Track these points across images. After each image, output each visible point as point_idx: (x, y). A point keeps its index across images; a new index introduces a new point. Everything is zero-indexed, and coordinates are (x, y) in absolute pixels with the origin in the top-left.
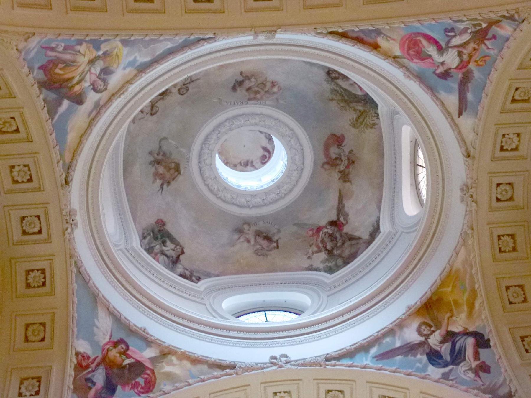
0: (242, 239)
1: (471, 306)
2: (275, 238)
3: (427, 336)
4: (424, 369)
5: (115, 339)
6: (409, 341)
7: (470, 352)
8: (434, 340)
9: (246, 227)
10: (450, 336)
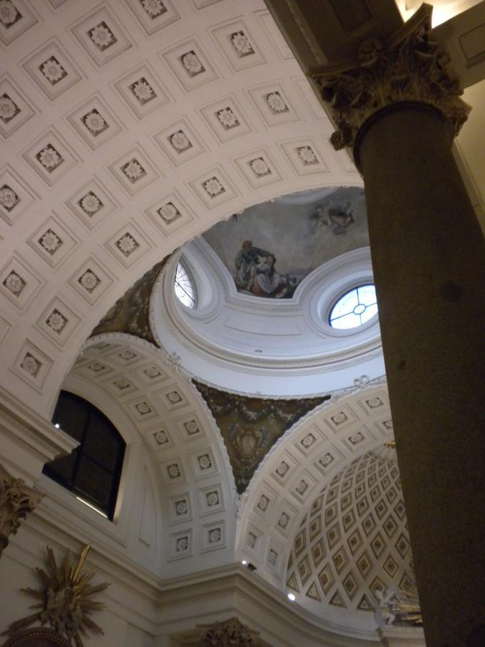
0: (320, 224)
2: (348, 212)
9: (319, 210)
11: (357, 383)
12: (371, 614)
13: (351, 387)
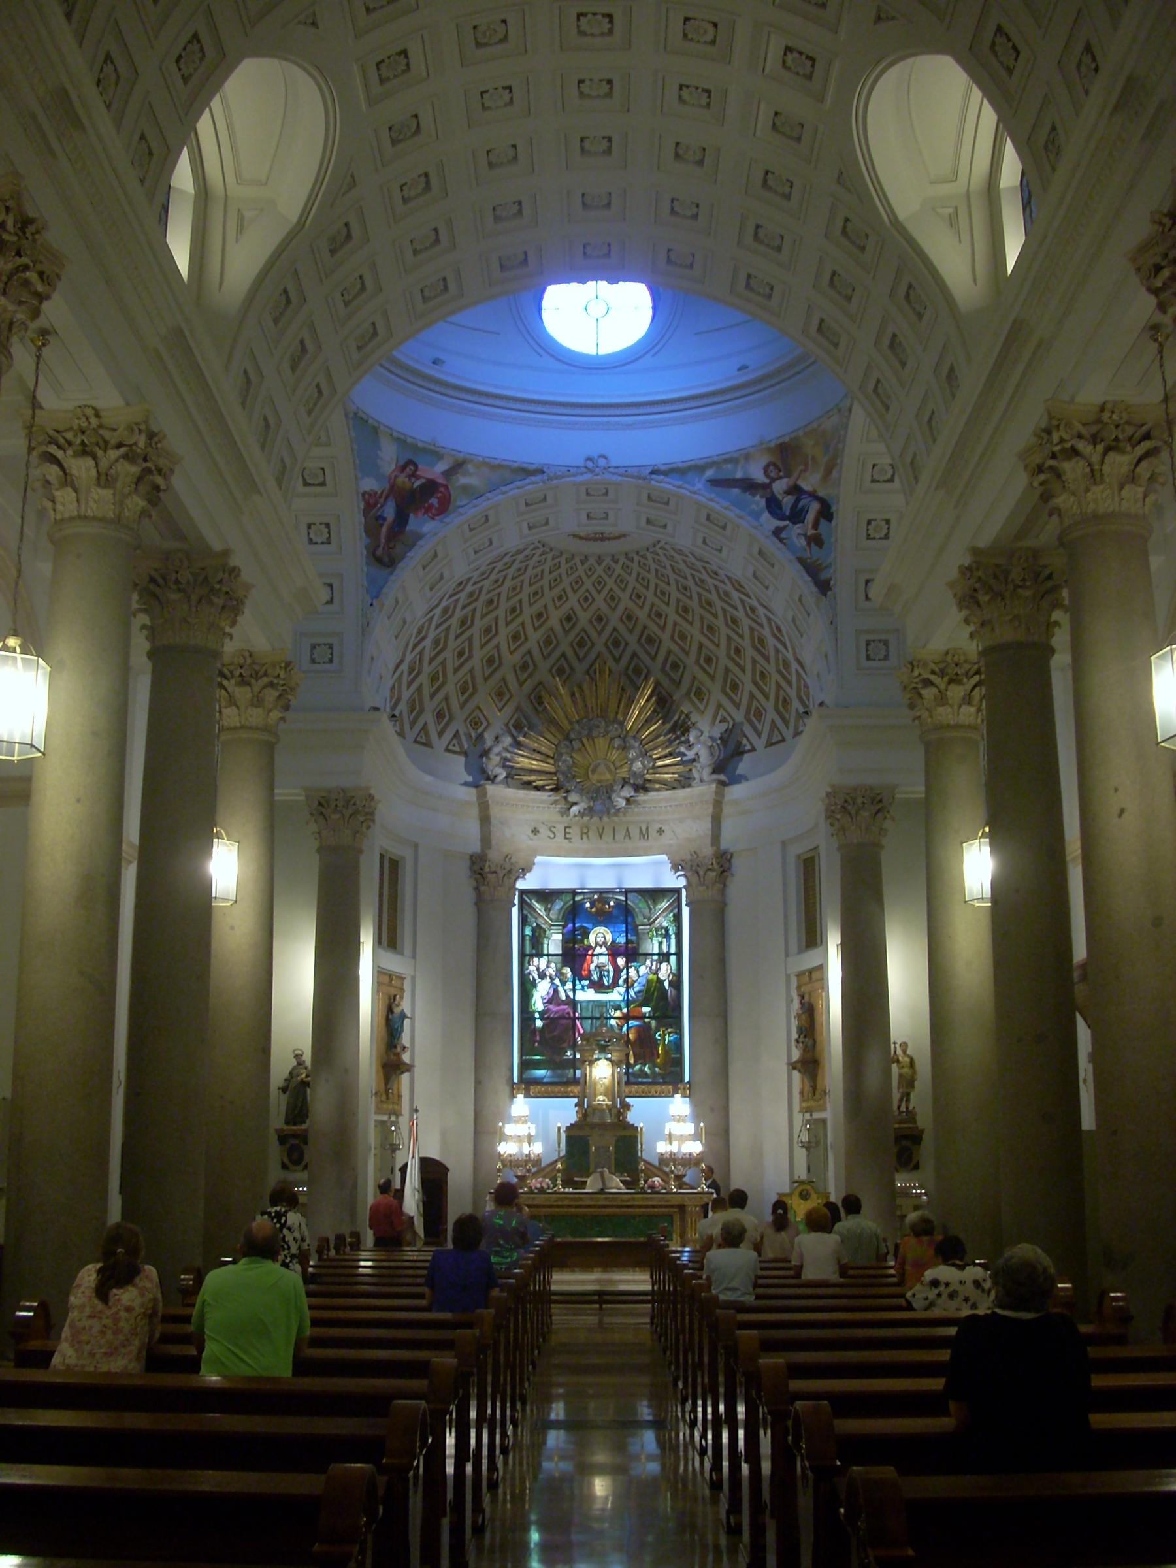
1: (828, 471)
3: (773, 480)
4: (757, 516)
5: (402, 463)
6: (753, 477)
7: (811, 517)
8: (779, 487)
10: (795, 490)
11: (590, 464)
12: (462, 759)
13: (578, 467)
